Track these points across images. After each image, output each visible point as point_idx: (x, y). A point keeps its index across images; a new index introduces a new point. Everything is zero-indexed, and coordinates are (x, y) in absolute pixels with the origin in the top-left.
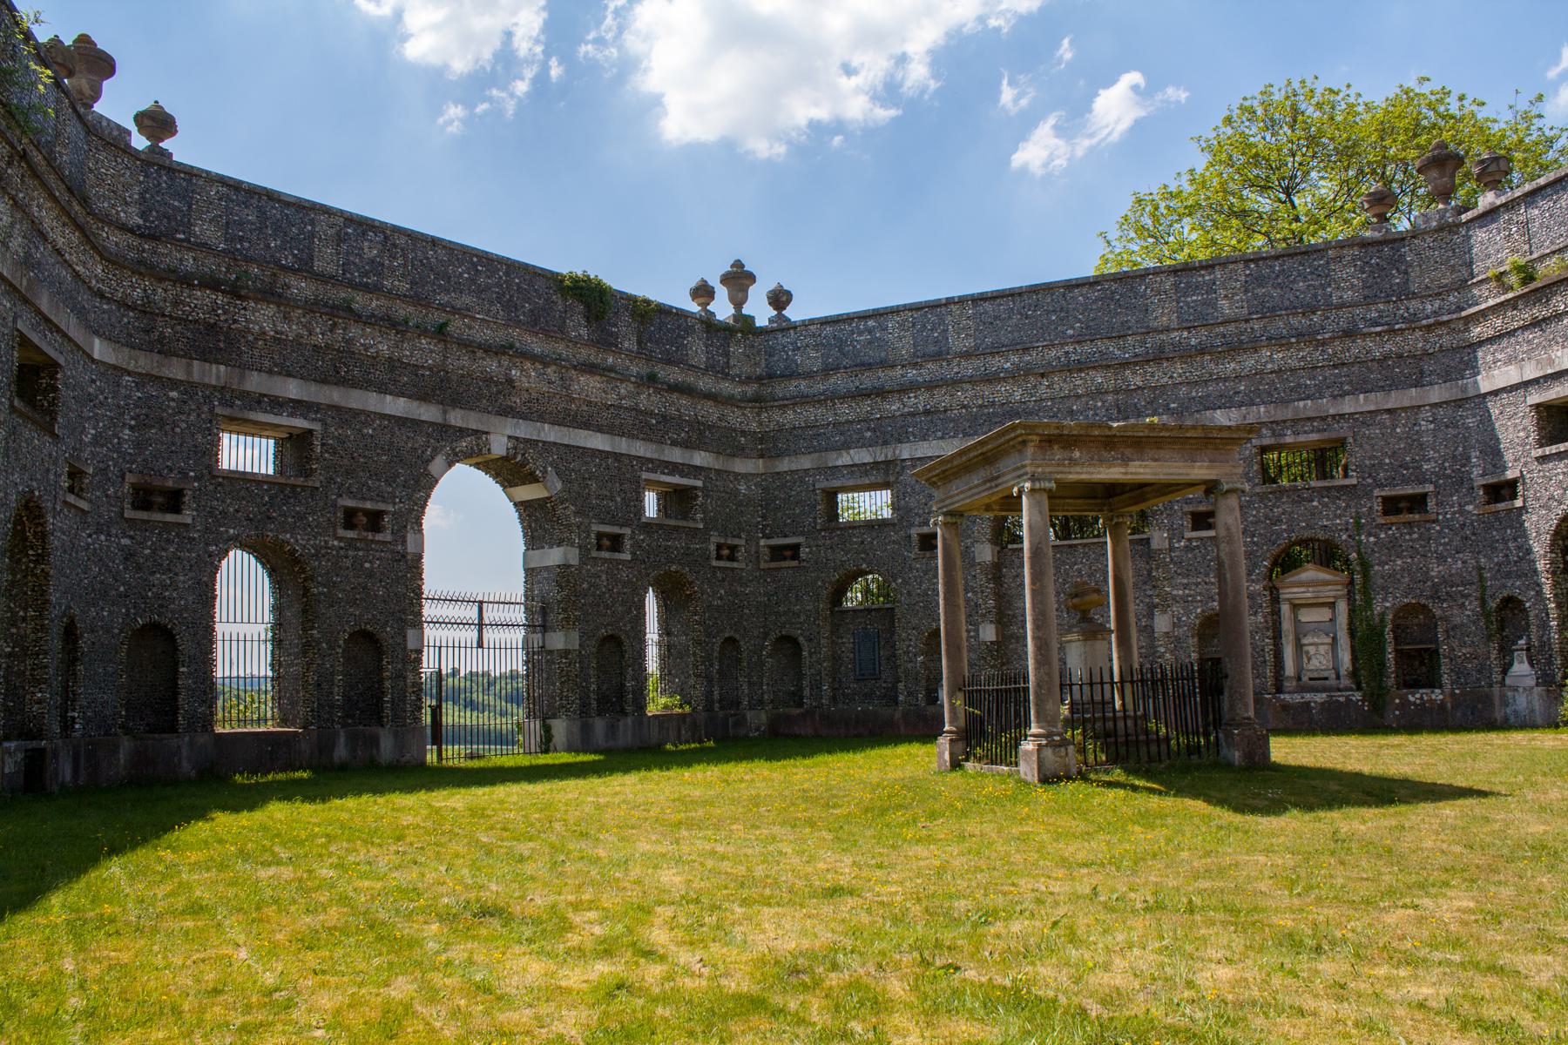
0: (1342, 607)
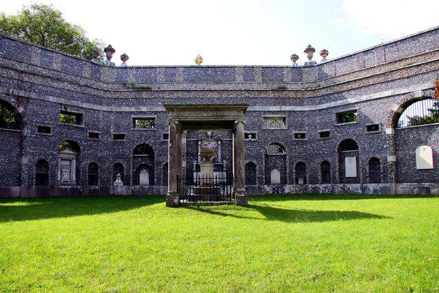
0: (74, 161)
